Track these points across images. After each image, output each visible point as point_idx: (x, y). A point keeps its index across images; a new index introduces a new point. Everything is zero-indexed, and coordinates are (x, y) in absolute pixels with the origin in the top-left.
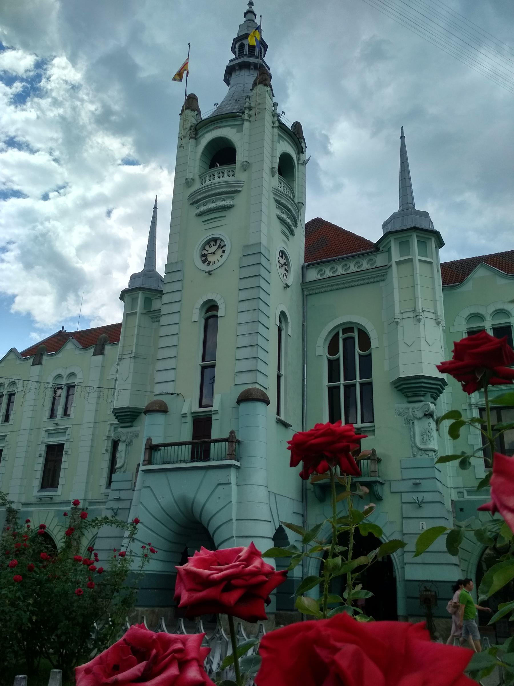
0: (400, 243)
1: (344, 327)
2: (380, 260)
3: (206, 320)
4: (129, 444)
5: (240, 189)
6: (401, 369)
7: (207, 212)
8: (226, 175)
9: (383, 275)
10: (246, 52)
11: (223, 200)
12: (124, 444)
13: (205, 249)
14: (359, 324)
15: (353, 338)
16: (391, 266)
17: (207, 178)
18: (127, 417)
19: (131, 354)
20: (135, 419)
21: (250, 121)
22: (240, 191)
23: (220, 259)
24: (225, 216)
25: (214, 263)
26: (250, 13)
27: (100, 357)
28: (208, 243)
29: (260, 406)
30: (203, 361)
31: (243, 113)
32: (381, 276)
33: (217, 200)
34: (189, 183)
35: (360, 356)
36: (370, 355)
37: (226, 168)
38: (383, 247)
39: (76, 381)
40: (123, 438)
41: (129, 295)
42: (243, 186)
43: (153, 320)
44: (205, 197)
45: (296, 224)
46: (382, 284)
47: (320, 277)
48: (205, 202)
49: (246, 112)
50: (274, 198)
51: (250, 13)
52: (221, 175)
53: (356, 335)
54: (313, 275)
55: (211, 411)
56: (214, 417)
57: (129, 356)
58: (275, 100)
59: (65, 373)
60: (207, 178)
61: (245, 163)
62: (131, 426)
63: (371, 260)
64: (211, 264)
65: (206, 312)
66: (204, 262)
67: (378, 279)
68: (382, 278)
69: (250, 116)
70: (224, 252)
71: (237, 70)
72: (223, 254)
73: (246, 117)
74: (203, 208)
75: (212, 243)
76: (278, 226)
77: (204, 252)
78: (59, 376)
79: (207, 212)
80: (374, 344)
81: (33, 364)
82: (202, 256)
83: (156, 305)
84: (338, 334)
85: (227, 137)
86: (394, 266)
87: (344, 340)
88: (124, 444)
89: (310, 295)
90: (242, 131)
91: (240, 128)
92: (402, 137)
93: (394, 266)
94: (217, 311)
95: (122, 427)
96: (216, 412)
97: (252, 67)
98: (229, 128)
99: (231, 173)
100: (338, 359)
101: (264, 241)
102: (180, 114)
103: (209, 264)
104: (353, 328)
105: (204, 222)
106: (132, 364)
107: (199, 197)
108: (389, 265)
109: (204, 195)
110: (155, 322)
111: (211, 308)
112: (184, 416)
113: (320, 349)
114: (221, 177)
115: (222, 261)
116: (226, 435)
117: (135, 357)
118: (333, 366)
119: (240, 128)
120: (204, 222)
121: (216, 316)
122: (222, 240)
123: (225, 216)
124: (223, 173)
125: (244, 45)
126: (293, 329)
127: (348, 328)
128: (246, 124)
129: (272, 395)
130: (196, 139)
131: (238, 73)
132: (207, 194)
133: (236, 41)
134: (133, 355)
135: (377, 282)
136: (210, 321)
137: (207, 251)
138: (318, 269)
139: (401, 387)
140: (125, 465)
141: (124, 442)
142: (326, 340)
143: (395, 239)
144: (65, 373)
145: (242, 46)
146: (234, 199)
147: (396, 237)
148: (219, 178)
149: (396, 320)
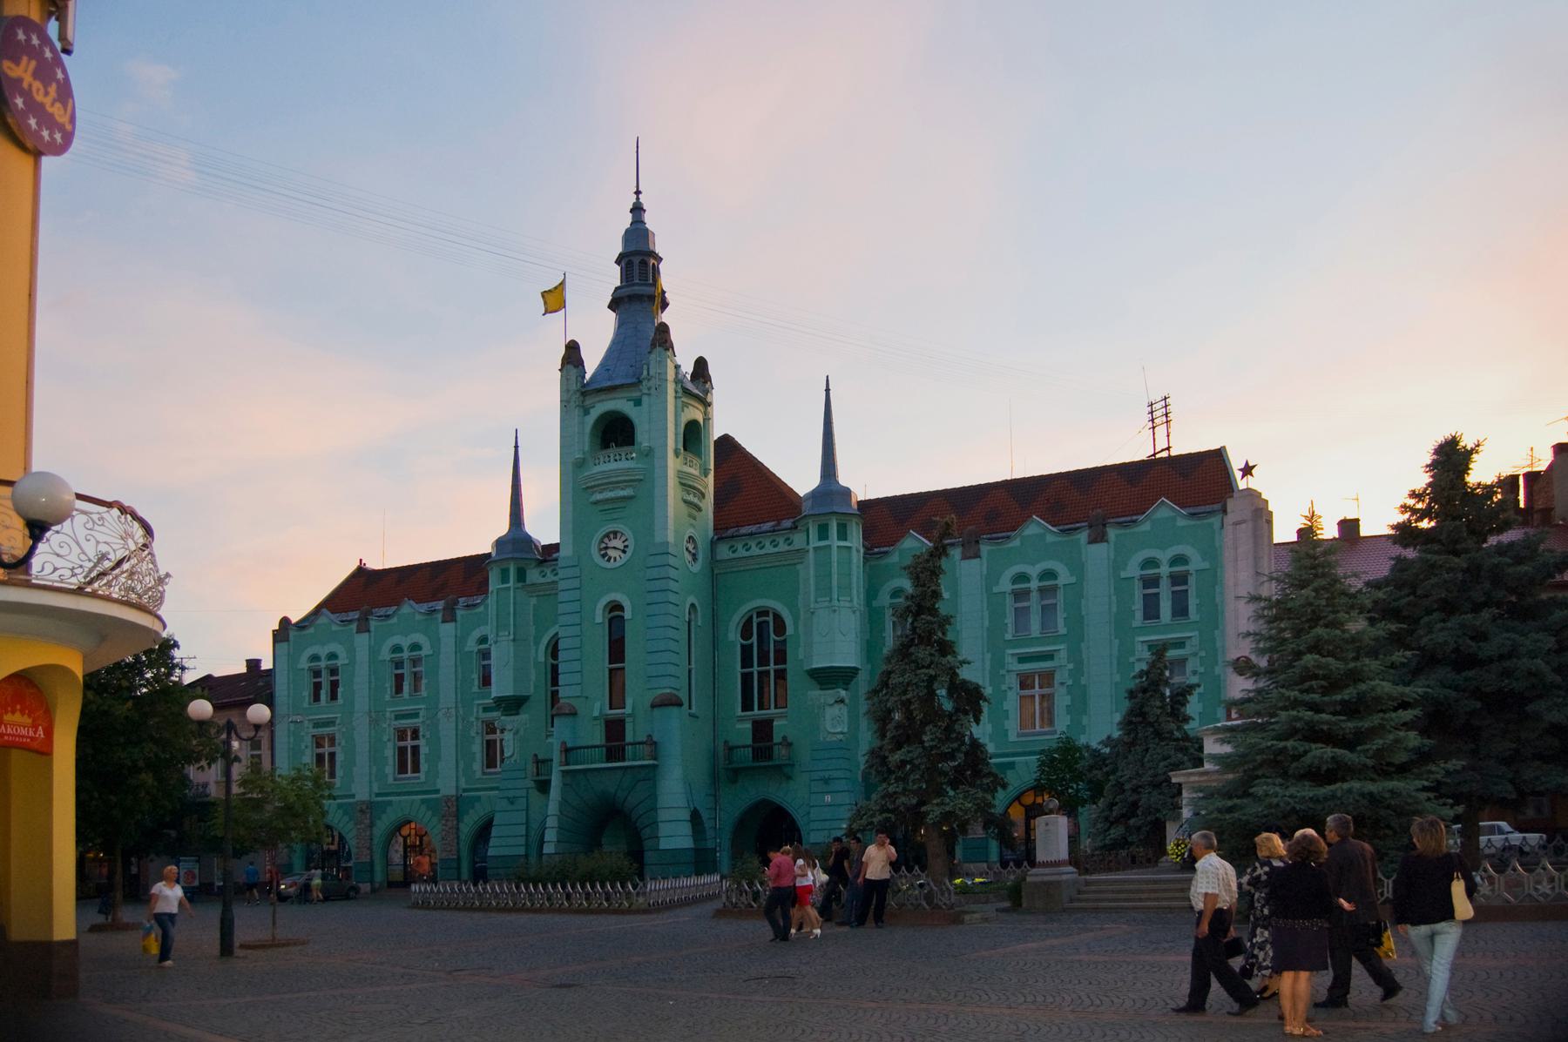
18: (513, 705)
27: (452, 625)
29: (675, 710)
31: (640, 382)
39: (423, 653)
45: (703, 495)
59: (405, 643)
73: (644, 387)
76: (684, 509)
78: (397, 649)
81: (359, 631)
83: (533, 576)
91: (638, 402)
100: (751, 645)
101: (671, 539)
111: (616, 607)
112: (596, 718)
113: (734, 636)
115: (625, 557)
118: (746, 652)
126: (700, 620)
128: (645, 399)
129: (683, 696)
144: (405, 643)
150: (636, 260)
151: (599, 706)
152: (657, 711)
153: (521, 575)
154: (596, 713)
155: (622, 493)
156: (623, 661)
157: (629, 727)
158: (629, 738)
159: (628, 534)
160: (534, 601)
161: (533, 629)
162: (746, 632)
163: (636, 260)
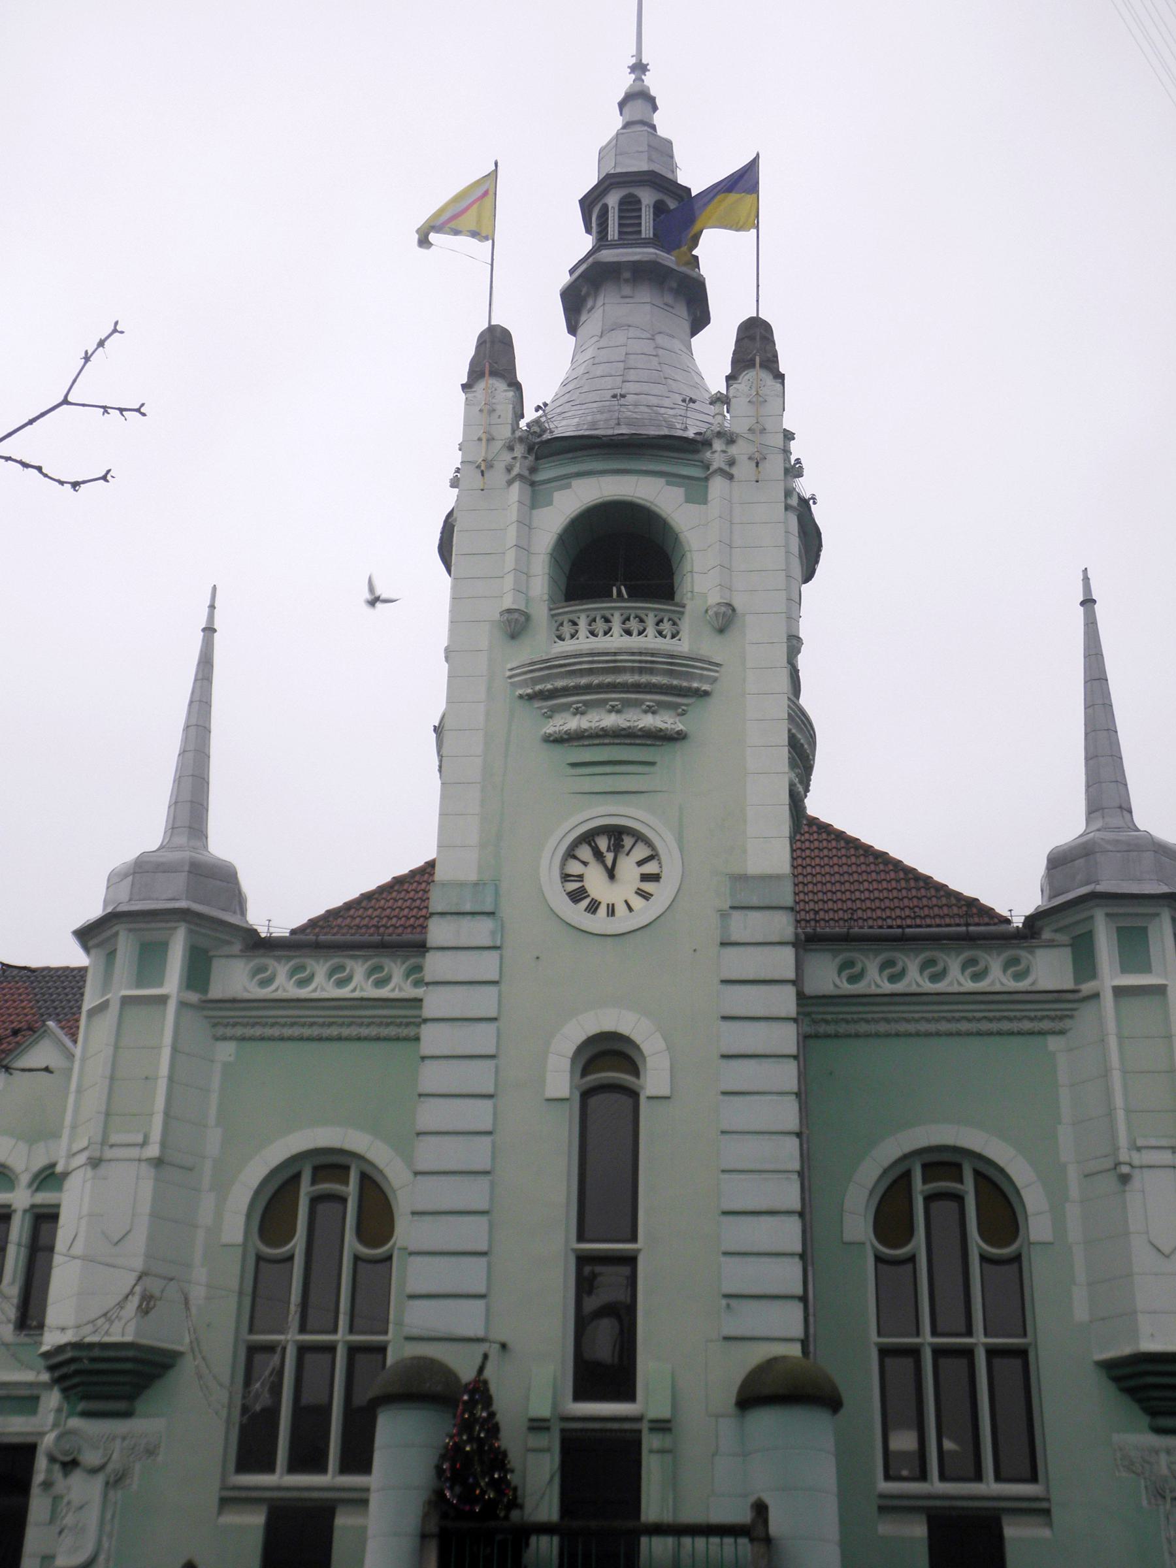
0: (1118, 928)
1: (928, 1158)
2: (1049, 970)
3: (586, 1095)
4: (117, 1481)
5: (705, 687)
6: (1145, 1324)
7: (591, 737)
8: (651, 631)
9: (1061, 1018)
10: (647, 227)
11: (650, 710)
12: (99, 1481)
13: (575, 857)
14: (980, 1157)
15: (959, 1199)
16: (1096, 996)
17: (583, 623)
19: (144, 1144)
20: (145, 1387)
21: (731, 477)
22: (706, 694)
23: (637, 903)
24: (653, 764)
25: (611, 910)
26: (639, 101)
28: (588, 838)
30: (581, 1238)
31: (707, 444)
32: (1052, 1019)
33: (628, 704)
34: (515, 626)
35: (984, 1258)
36: (1017, 1259)
37: (650, 610)
38: (1056, 931)
40: (90, 1458)
41: (130, 930)
42: (715, 680)
43: (220, 1031)
44: (588, 689)
46: (1053, 1043)
47: (847, 988)
48: (585, 703)
49: (718, 445)
50: (789, 731)
51: (639, 101)
52: (634, 625)
53: (968, 1187)
54: (825, 976)
55: (639, 1419)
56: (650, 1442)
57: (134, 1152)
58: (787, 425)
60: (583, 623)
61: (723, 609)
62: (127, 1414)
63: (1015, 961)
64: (602, 911)
65: (585, 1072)
66: (577, 896)
67: (1045, 1025)
68: (1058, 1025)
69: (732, 463)
70: (655, 878)
71: (627, 281)
72: (648, 887)
73: (717, 456)
74: (573, 723)
75: (603, 843)
77: (574, 868)
79: (591, 737)
80: (1038, 1226)
82: (566, 877)
84: (907, 1175)
85: (654, 508)
86: (1108, 998)
87: (929, 1199)
88: (99, 1481)
89: (817, 1036)
90: (705, 501)
91: (697, 491)
92: (1088, 602)
93: (1108, 998)
94: (636, 1072)
95: (86, 1414)
96: (662, 1426)
97: (674, 285)
98: (661, 482)
99: (666, 627)
100: (912, 1259)
102: (464, 387)
103: (593, 907)
104: (959, 1166)
105: (574, 765)
106: (147, 1188)
107: (560, 683)
108: (1087, 988)
109: (583, 681)
110: (224, 1038)
112: (537, 1425)
113: (858, 1225)
114: (635, 633)
116: (743, 1516)
117: (158, 1163)
119: (697, 491)
120: (574, 765)
121: (633, 1094)
122: (639, 837)
123: (653, 764)
124: (642, 621)
125: (639, 202)
127: (943, 1163)
128: (717, 485)
130: (533, 484)
131: (627, 290)
132: (596, 680)
133: (607, 183)
134: (153, 1151)
135: (1041, 1033)
136: (593, 1101)
137: (585, 864)
138: (839, 959)
139: (1132, 1383)
140: (102, 1558)
141: (94, 1471)
142: (871, 1192)
143: (1107, 915)
145: (630, 205)
146: (684, 713)
147: (1109, 910)
148: (629, 633)
149: (1125, 1169)
150: (648, 198)
151: (535, 1386)
152: (765, 1420)
153: (198, 971)
154: (541, 1408)
155: (648, 721)
156: (634, 1238)
157: (652, 1470)
158: (652, 1509)
159: (666, 843)
160: (226, 1051)
161: (214, 1138)
162: (892, 1216)
163: (648, 198)
